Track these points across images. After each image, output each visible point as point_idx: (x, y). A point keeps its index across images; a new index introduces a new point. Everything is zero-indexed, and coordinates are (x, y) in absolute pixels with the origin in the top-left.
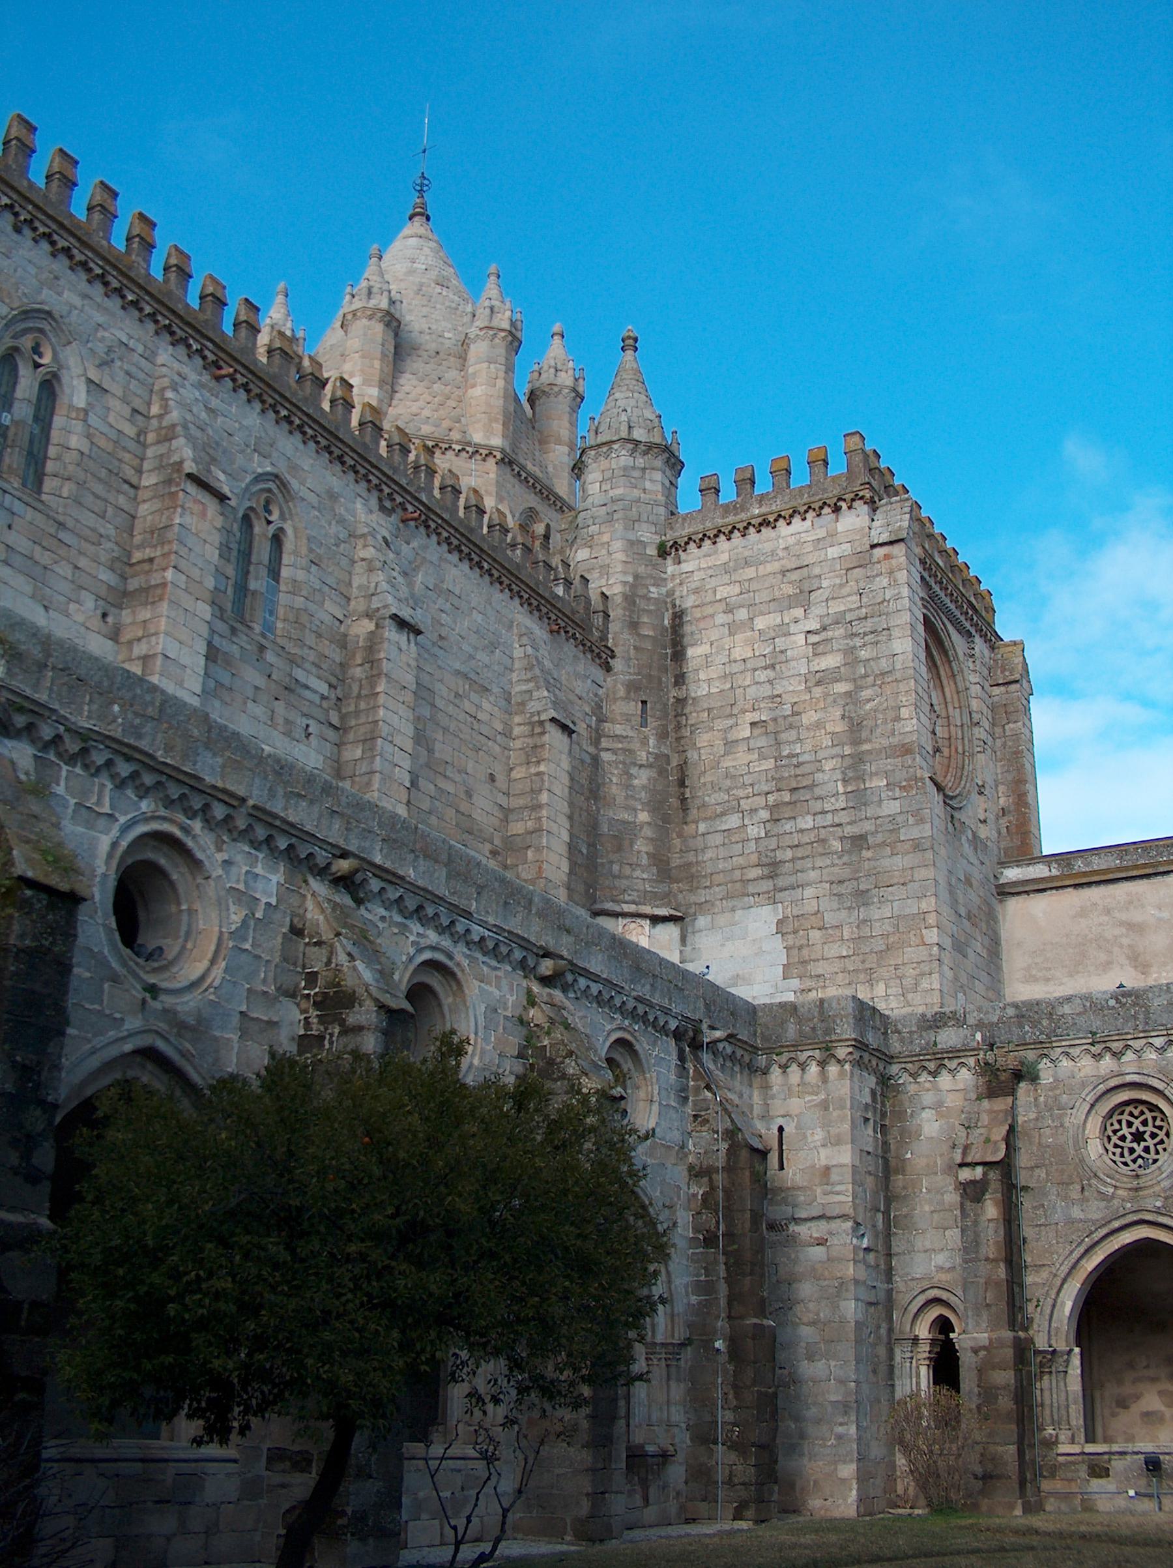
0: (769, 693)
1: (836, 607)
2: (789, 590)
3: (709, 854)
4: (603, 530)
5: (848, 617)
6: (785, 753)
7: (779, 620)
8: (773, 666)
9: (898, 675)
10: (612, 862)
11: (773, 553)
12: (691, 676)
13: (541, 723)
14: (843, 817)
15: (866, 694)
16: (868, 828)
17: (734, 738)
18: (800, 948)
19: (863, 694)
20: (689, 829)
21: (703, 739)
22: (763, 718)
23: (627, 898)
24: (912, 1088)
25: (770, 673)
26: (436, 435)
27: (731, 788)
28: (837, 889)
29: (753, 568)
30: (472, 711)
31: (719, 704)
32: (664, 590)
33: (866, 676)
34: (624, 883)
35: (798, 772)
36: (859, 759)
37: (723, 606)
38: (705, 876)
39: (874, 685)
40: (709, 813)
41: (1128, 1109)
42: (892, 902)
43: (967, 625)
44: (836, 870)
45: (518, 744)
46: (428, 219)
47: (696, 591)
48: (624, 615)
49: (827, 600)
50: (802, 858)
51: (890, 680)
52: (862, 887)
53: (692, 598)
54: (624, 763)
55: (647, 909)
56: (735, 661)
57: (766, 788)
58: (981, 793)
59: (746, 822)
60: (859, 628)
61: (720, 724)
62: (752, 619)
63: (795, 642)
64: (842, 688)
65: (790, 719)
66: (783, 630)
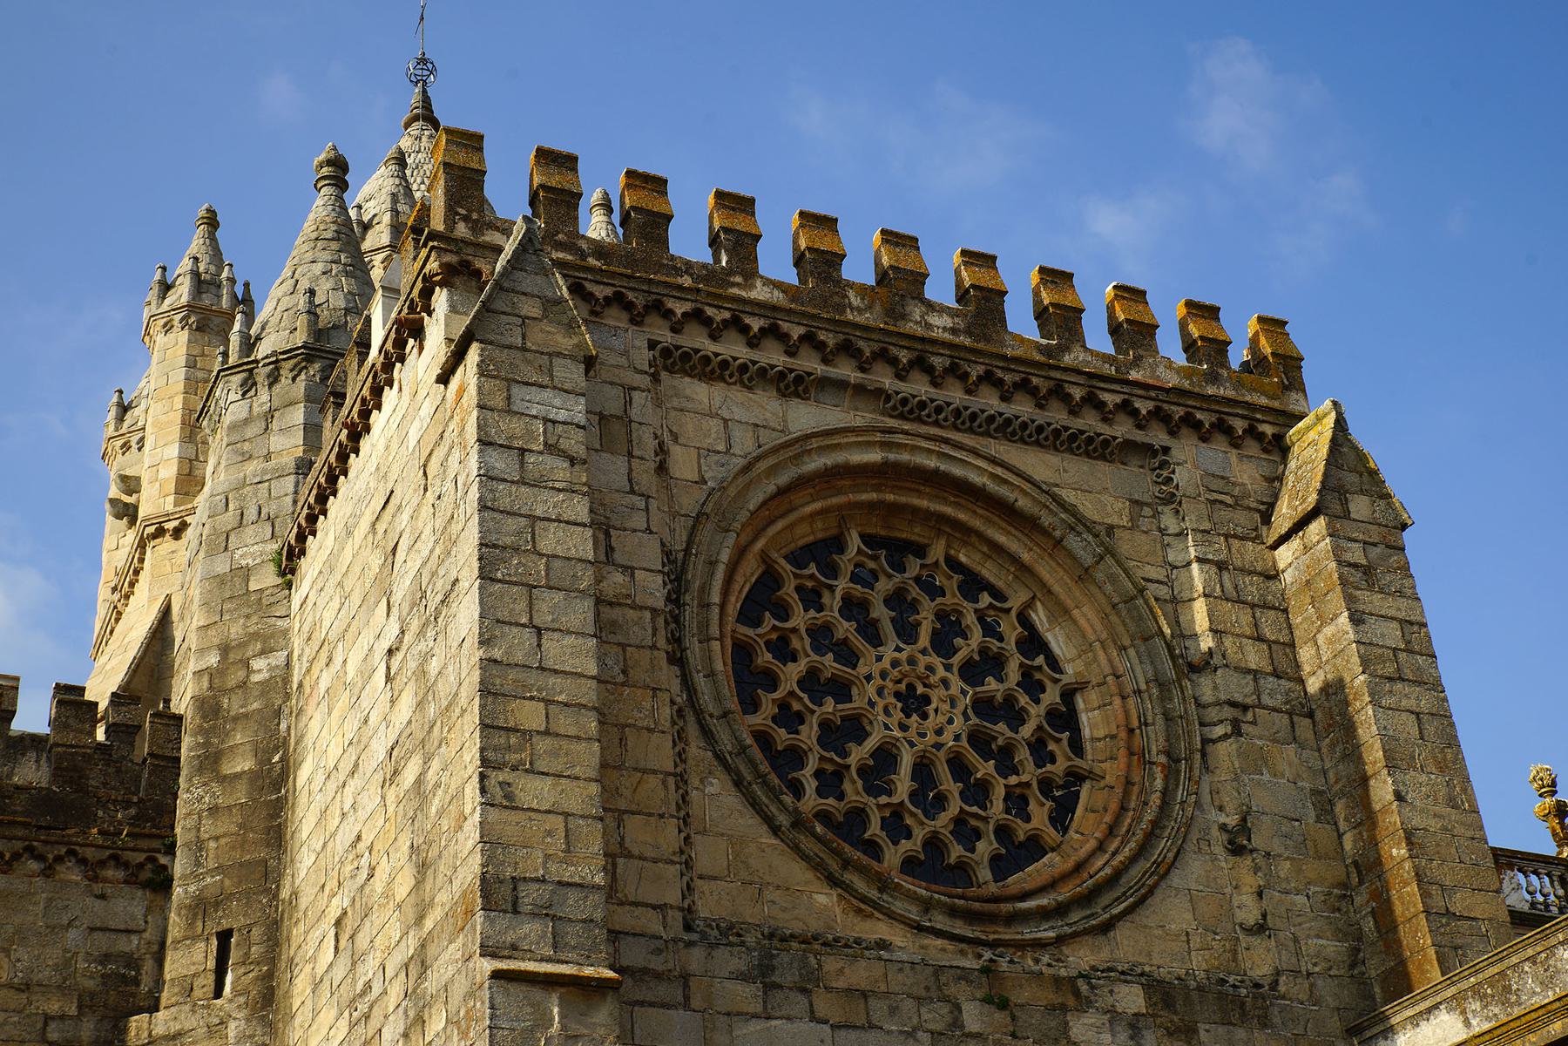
21: (300, 988)
32: (279, 658)
43: (1122, 429)
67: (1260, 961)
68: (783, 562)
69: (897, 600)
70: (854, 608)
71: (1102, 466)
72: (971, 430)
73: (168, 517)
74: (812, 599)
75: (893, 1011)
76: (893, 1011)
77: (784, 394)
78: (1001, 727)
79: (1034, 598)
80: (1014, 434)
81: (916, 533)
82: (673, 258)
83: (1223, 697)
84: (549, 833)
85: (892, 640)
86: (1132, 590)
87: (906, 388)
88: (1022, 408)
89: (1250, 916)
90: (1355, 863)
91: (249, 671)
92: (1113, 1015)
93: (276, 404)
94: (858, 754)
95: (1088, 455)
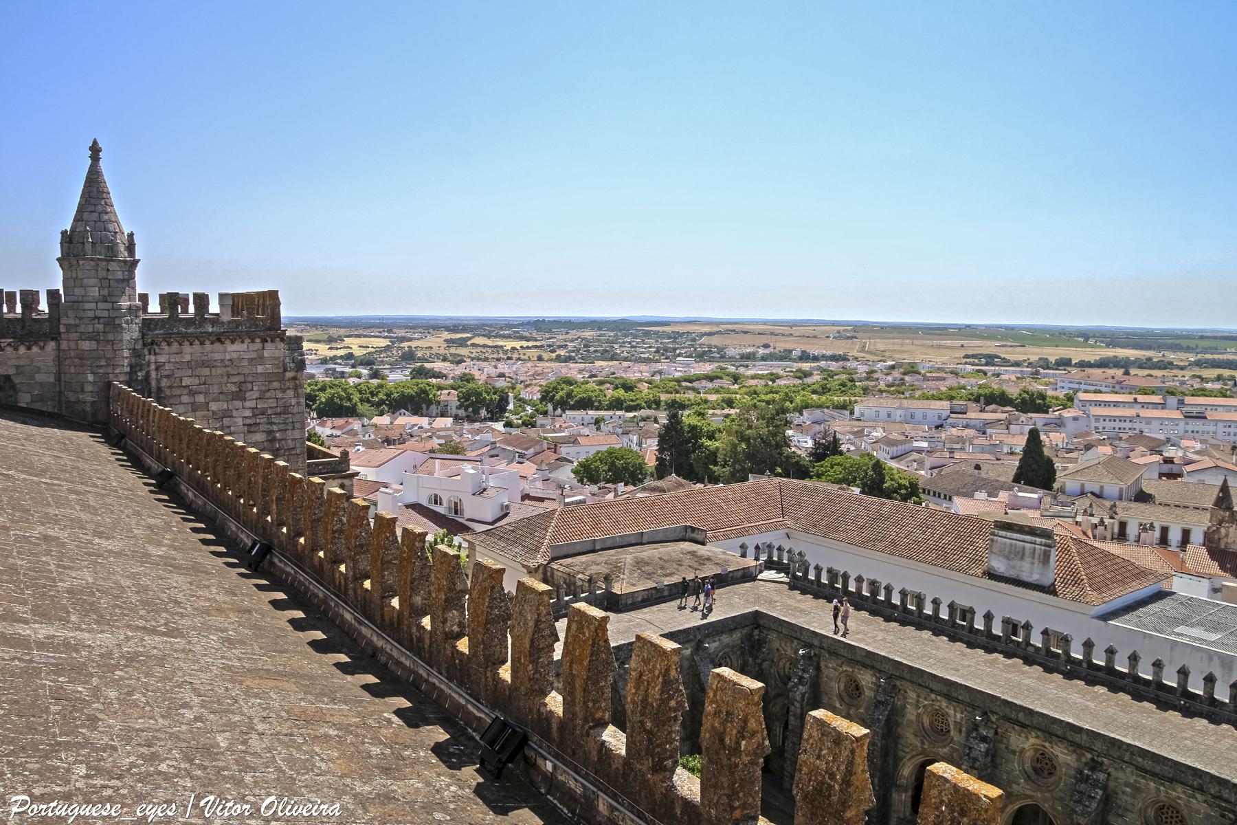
2: (234, 389)
4: (107, 330)
5: (269, 412)
7: (225, 406)
9: (298, 451)
11: (222, 361)
29: (208, 369)
33: (278, 450)
47: (167, 376)
49: (256, 399)
51: (293, 452)
53: (165, 380)
60: (275, 419)
62: (208, 404)
63: (236, 422)
66: (227, 414)
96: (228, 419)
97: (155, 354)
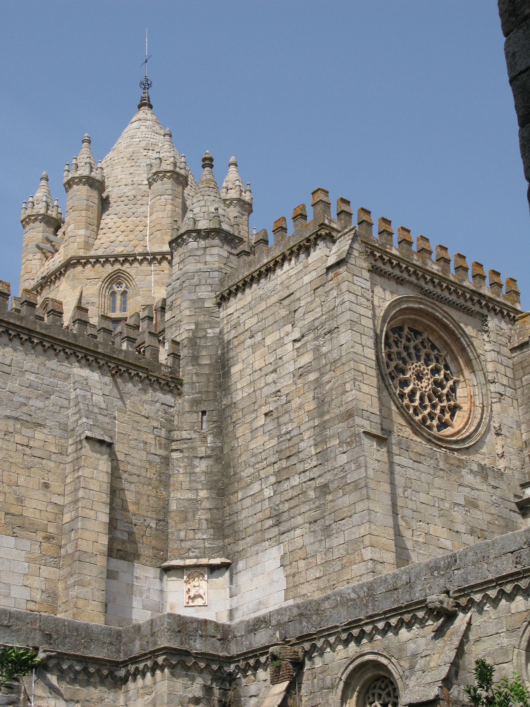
0: (274, 390)
1: (310, 318)
2: (284, 312)
3: (245, 513)
5: (317, 323)
6: (283, 432)
7: (278, 337)
8: (275, 371)
9: (344, 360)
10: (180, 530)
12: (233, 388)
13: (81, 441)
14: (315, 473)
15: (326, 378)
16: (329, 477)
17: (256, 427)
18: (294, 576)
19: (324, 378)
20: (233, 498)
22: (271, 409)
23: (191, 554)
24: (244, 681)
25: (274, 375)
26: (125, 252)
27: (255, 464)
28: (314, 527)
29: (264, 303)
30: (25, 441)
31: (248, 404)
32: (217, 330)
34: (189, 544)
35: (291, 443)
36: (323, 426)
37: (248, 334)
38: (242, 531)
39: (330, 370)
40: (243, 484)
41: (378, 683)
42: (344, 531)
43: (477, 308)
44: (312, 513)
45: (69, 459)
46: (151, 107)
48: (189, 353)
50: (294, 507)
52: (327, 523)
54: (188, 457)
55: (204, 561)
56: (256, 371)
57: (273, 460)
58: (498, 434)
59: (264, 487)
61: (249, 418)
64: (312, 377)
65: (286, 406)
67: (501, 464)
68: (390, 332)
69: (415, 348)
70: (406, 348)
71: (470, 317)
72: (440, 302)
73: (83, 258)
74: (396, 343)
75: (425, 459)
76: (425, 459)
77: (397, 283)
78: (439, 389)
79: (448, 353)
80: (451, 305)
81: (419, 329)
82: (373, 238)
83: (497, 391)
84: (368, 399)
85: (415, 360)
86: (476, 357)
87: (426, 287)
88: (453, 298)
89: (500, 451)
90: (525, 442)
91: (207, 333)
92: (471, 471)
93: (207, 246)
94: (407, 390)
95: (467, 314)
96: (281, 349)
97: (226, 309)
